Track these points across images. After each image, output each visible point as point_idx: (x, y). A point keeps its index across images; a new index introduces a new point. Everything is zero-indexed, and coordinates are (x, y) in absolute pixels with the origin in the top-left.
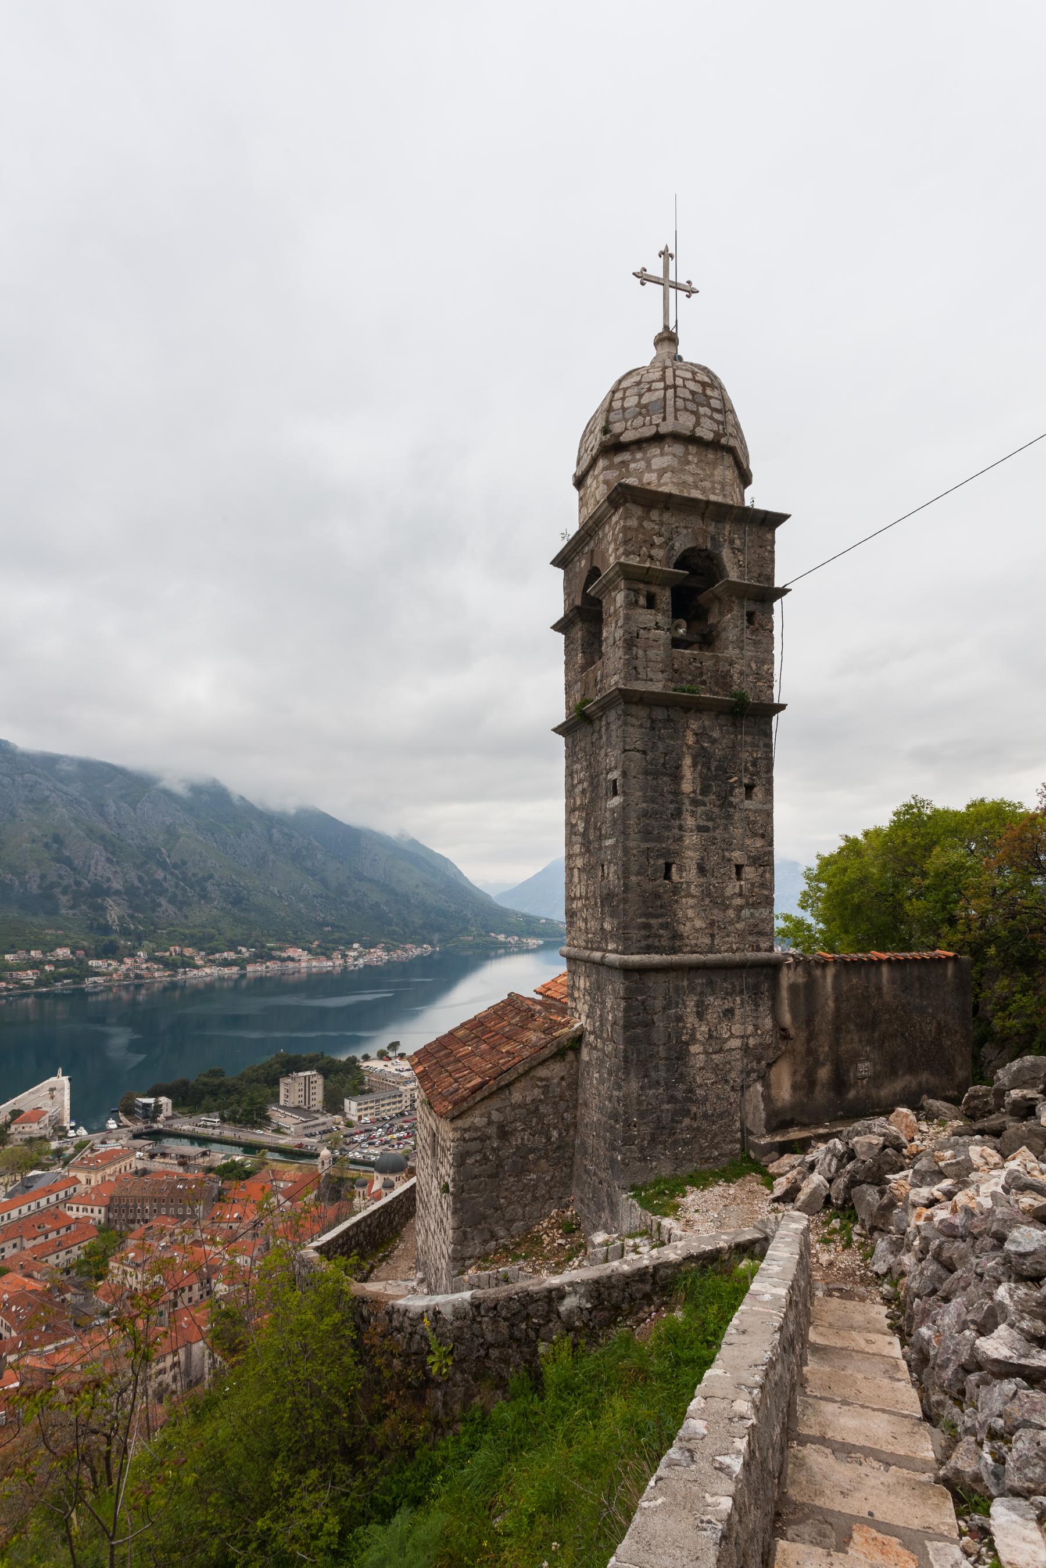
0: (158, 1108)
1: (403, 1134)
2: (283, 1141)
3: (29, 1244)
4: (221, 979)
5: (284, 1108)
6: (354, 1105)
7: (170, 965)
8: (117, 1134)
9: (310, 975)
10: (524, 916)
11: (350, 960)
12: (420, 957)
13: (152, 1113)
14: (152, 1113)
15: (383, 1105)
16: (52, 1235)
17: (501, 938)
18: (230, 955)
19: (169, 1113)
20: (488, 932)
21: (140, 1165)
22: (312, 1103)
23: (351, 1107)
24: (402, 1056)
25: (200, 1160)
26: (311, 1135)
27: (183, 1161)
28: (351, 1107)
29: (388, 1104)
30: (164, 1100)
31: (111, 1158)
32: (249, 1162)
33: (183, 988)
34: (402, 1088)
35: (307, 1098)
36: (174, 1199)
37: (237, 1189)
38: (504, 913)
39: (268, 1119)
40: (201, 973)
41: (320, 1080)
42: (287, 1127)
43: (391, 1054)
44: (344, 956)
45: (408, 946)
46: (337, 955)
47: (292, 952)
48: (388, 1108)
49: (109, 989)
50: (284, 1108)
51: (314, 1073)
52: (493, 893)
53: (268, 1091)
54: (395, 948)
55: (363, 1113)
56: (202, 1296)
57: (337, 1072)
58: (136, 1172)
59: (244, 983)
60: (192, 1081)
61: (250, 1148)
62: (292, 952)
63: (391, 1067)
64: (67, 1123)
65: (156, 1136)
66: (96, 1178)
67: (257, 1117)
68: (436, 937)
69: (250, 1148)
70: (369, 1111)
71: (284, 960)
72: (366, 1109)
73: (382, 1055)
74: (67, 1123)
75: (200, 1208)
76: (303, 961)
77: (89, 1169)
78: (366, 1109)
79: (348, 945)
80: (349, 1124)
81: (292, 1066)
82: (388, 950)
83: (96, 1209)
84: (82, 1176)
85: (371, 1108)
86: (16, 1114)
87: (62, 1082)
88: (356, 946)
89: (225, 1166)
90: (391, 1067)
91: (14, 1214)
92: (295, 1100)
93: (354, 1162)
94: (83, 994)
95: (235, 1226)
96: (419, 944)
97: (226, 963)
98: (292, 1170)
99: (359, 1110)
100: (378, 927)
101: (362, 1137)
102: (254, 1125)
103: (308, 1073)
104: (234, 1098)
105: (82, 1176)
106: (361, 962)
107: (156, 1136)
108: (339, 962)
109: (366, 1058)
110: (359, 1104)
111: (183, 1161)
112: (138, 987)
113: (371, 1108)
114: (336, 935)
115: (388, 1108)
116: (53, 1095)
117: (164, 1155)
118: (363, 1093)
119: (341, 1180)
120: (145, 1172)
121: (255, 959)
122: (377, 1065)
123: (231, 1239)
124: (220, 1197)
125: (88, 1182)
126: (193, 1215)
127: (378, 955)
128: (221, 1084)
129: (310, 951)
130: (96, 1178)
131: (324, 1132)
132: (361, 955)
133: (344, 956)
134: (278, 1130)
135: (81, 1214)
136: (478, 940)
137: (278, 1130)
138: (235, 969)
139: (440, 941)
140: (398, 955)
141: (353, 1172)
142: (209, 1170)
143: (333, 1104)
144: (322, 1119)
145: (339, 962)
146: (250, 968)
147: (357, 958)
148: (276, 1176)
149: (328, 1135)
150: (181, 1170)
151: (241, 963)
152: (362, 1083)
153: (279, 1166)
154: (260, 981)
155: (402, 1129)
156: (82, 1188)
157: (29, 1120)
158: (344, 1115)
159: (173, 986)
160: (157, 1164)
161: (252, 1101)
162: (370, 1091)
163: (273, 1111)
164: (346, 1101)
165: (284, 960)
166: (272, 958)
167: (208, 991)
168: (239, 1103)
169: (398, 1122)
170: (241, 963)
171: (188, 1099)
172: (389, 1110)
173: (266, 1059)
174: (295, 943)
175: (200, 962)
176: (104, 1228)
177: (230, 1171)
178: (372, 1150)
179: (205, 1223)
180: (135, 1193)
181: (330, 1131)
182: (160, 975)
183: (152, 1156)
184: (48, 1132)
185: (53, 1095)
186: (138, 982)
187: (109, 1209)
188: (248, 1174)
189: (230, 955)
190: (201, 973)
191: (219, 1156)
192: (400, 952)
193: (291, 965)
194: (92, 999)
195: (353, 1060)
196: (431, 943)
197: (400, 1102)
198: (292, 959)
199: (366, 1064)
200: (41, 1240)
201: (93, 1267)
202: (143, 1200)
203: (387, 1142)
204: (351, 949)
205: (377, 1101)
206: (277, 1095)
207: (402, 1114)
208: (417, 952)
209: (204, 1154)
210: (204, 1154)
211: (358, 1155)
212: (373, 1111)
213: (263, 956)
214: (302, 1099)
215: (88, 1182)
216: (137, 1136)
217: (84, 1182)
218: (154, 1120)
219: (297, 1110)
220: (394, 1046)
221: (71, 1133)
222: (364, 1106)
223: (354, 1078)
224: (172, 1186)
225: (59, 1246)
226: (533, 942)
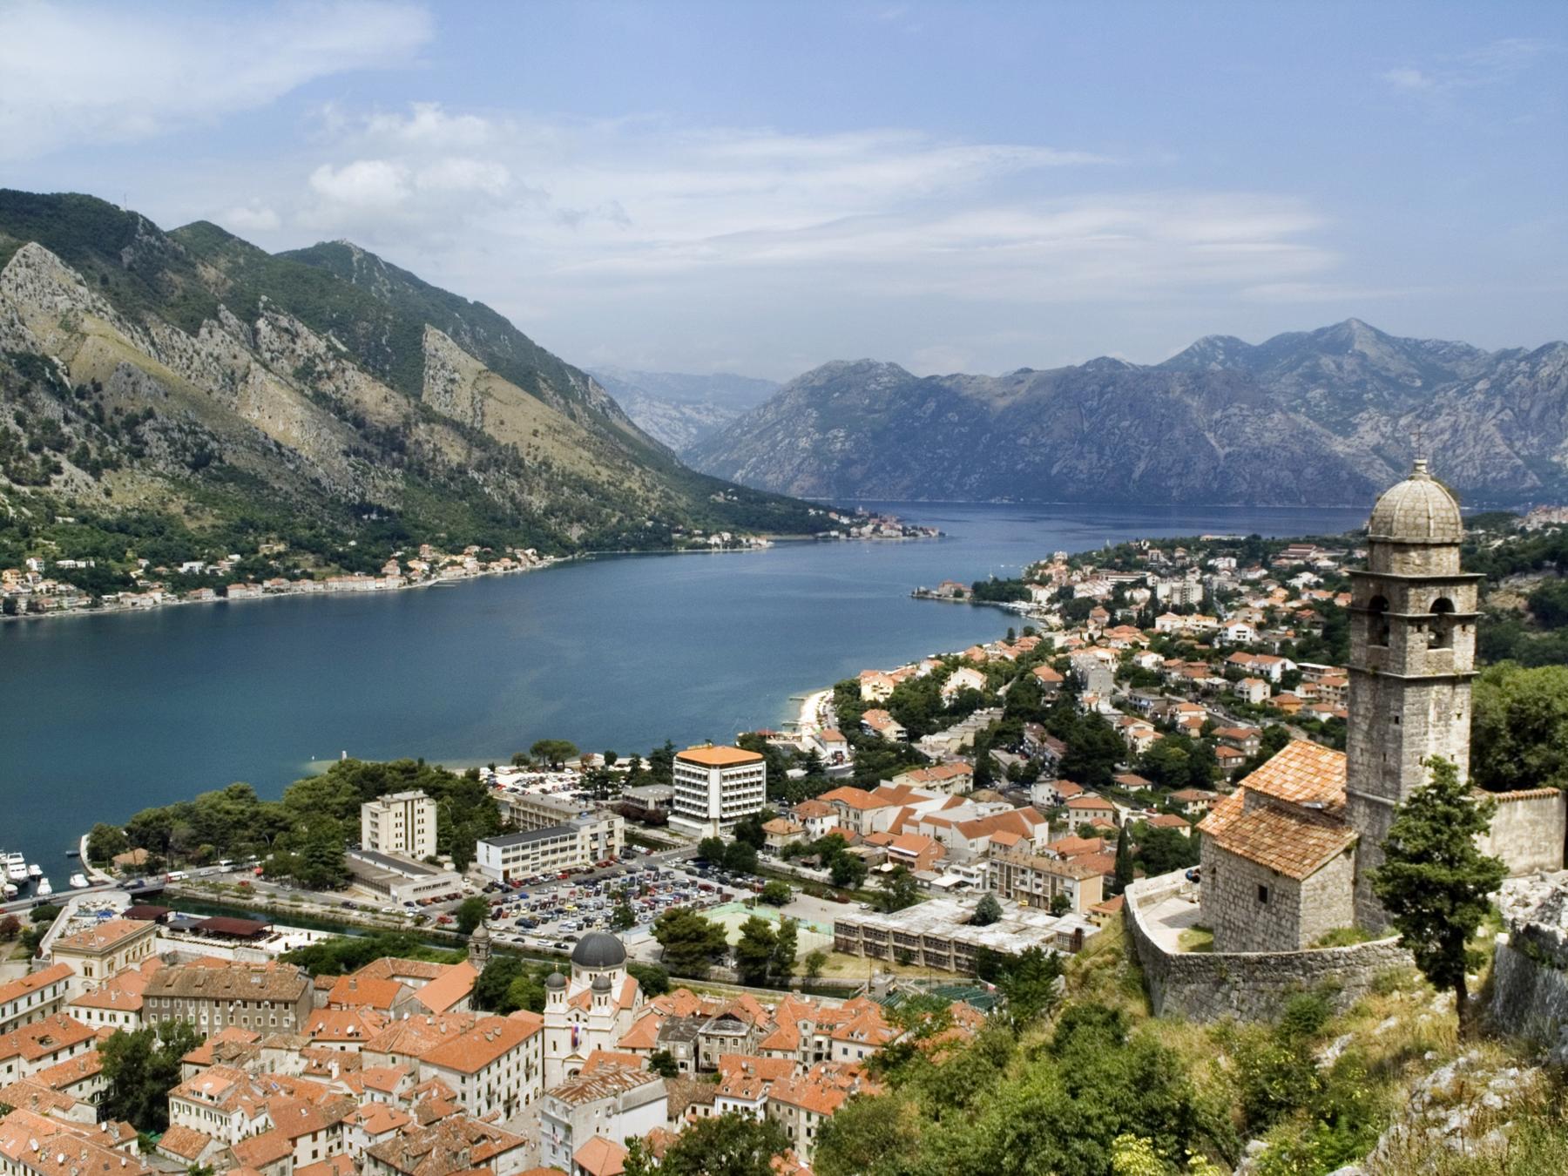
6: (496, 853)
15: (545, 853)
22: (418, 847)
29: (554, 851)
35: (410, 838)
44: (405, 570)
46: (391, 567)
48: (554, 857)
51: (421, 793)
55: (510, 866)
56: (331, 1149)
58: (164, 957)
67: (327, 871)
70: (521, 863)
72: (516, 859)
78: (516, 859)
81: (375, 785)
83: (120, 1016)
85: (525, 857)
99: (505, 861)
103: (408, 795)
105: (76, 964)
110: (504, 851)
113: (525, 857)
115: (554, 857)
121: (240, 575)
125: (88, 971)
156: (77, 988)
192: (507, 562)
197: (573, 848)
200: (48, 1062)
205: (535, 846)
212: (528, 862)
214: (402, 840)
215: (88, 971)
217: (80, 971)
222: (511, 855)
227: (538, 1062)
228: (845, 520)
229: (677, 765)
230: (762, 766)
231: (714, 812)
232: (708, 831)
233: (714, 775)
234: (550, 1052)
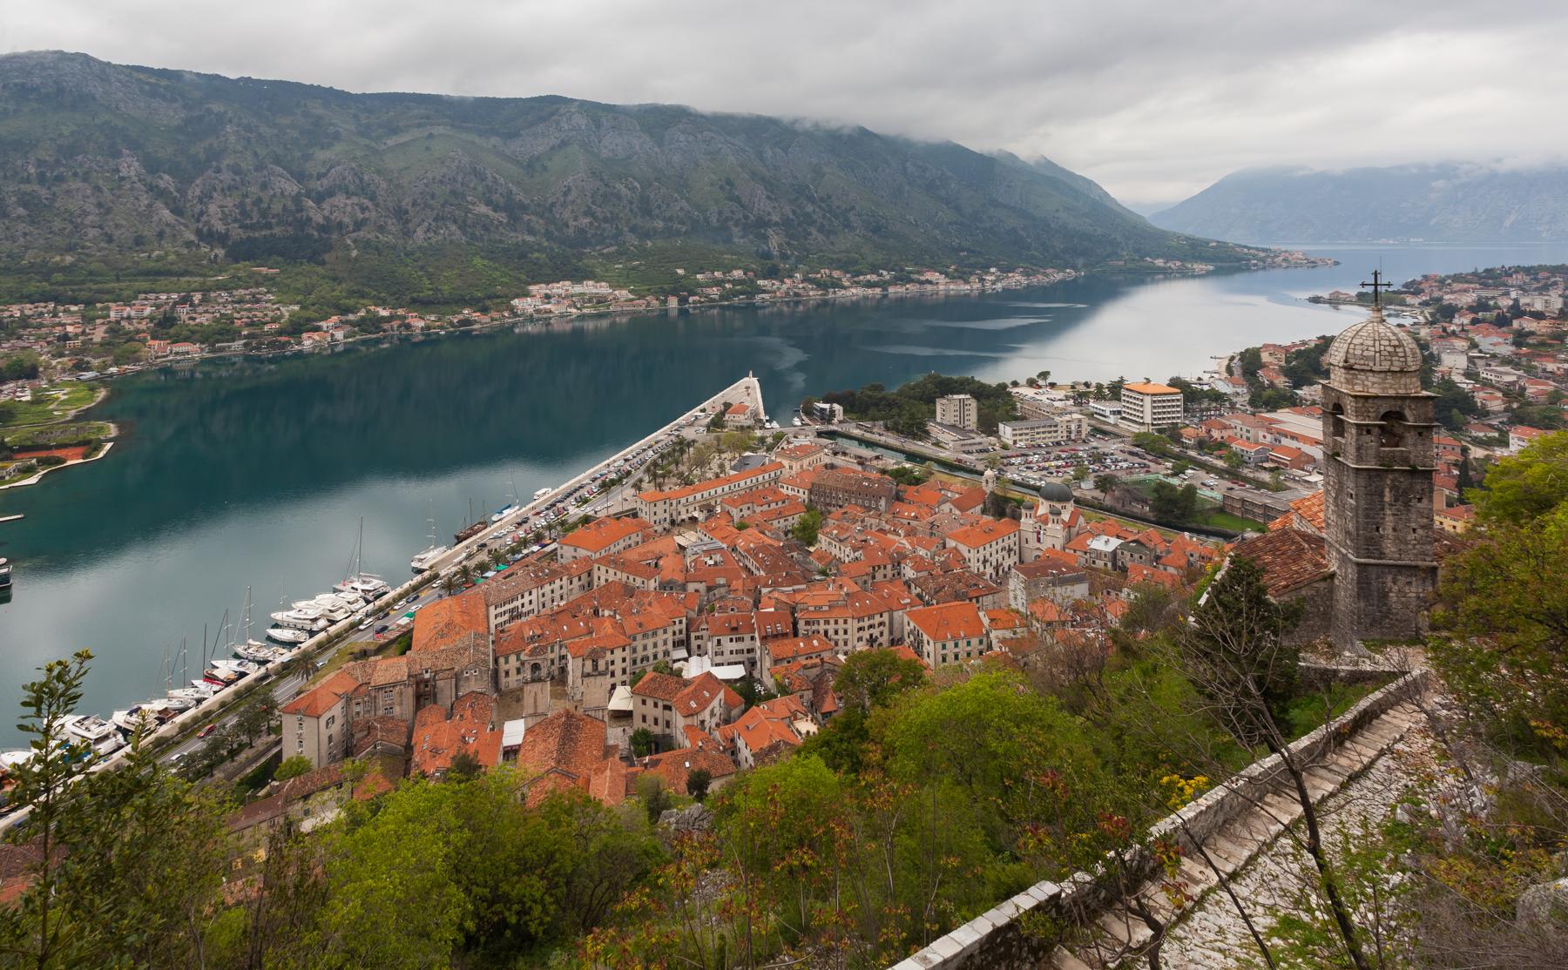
0: (832, 413)
1: (1060, 463)
2: (943, 455)
3: (758, 509)
4: (866, 298)
5: (941, 424)
6: (1008, 430)
7: (820, 285)
8: (802, 433)
9: (947, 296)
10: (1187, 238)
11: (988, 285)
12: (1062, 282)
13: (827, 417)
14: (827, 417)
16: (773, 506)
17: (1160, 262)
18: (873, 278)
19: (841, 417)
20: (1142, 258)
21: (827, 460)
23: (1006, 431)
24: (1053, 385)
25: (875, 462)
26: (969, 453)
27: (861, 461)
28: (1006, 431)
30: (836, 407)
31: (805, 451)
32: (917, 470)
33: (834, 305)
34: (1057, 419)
35: (962, 417)
36: (863, 495)
37: (910, 491)
38: (1162, 236)
39: (927, 433)
40: (848, 293)
41: (973, 404)
42: (945, 442)
43: (1041, 383)
44: (982, 280)
45: (1049, 271)
47: (929, 276)
49: (774, 303)
50: (941, 424)
52: (1146, 215)
53: (925, 408)
54: (1035, 273)
57: (988, 397)
58: (826, 466)
59: (886, 302)
60: (858, 394)
61: (911, 456)
62: (929, 276)
63: (1044, 396)
64: (764, 417)
65: (832, 435)
66: (796, 466)
68: (1080, 261)
69: (911, 456)
71: (922, 283)
73: (1031, 383)
74: (764, 417)
75: (883, 502)
76: (941, 284)
77: (791, 458)
79: (985, 268)
80: (1005, 447)
81: (947, 388)
82: (1027, 275)
84: (786, 463)
86: (727, 406)
87: (752, 381)
88: (993, 270)
89: (897, 471)
90: (1044, 396)
91: (742, 484)
92: (951, 418)
93: (1014, 483)
94: (752, 308)
95: (914, 523)
96: (1061, 268)
97: (870, 285)
98: (958, 482)
100: (1014, 252)
101: (1019, 460)
102: (915, 437)
104: (895, 411)
105: (786, 463)
106: (999, 286)
107: (832, 435)
108: (977, 286)
109: (1015, 384)
111: (861, 461)
112: (797, 303)
114: (972, 260)
116: (747, 392)
117: (845, 454)
118: (1016, 419)
119: (1007, 500)
120: (832, 467)
122: (1029, 392)
123: (911, 533)
124: (898, 498)
126: (877, 509)
127: (1017, 279)
128: (883, 398)
129: (947, 275)
130: (796, 466)
131: (981, 451)
132: (998, 280)
133: (982, 280)
134: (937, 444)
135: (790, 493)
136: (1130, 265)
137: (937, 444)
138: (878, 290)
139: (1085, 266)
140: (1038, 279)
141: (1015, 494)
142: (884, 472)
143: (988, 425)
144: (978, 439)
145: (977, 286)
146: (891, 290)
147: (994, 281)
148: (945, 486)
149: (985, 455)
150: (859, 468)
151: (883, 285)
152: (1015, 409)
153: (944, 477)
154: (901, 300)
155: (1058, 458)
156: (786, 471)
157: (736, 412)
158: (999, 437)
159: (825, 303)
160: (839, 461)
161: (912, 416)
162: (1023, 418)
163: (932, 428)
164: (1001, 426)
165: (922, 283)
166: (912, 281)
167: (855, 307)
168: (899, 415)
169: (1056, 452)
170: (883, 285)
171: (857, 407)
172: (1045, 439)
173: (920, 378)
174: (932, 268)
175: (847, 284)
176: (810, 507)
177: (900, 475)
178: (1030, 474)
179: (889, 516)
180: (830, 483)
181: (986, 451)
182: (814, 294)
183: (835, 454)
184: (751, 422)
185: (747, 392)
186: (797, 299)
187: (811, 492)
188: (917, 481)
189: (873, 278)
190: (848, 293)
191: (891, 462)
193: (929, 287)
194: (760, 312)
195: (1003, 387)
196: (1074, 268)
198: (930, 282)
199: (1015, 390)
200: (765, 508)
201: (807, 535)
202: (837, 489)
203: (1044, 469)
204: (988, 273)
206: (934, 412)
207: (1058, 444)
208: (1059, 276)
209: (877, 458)
210: (877, 458)
211: (1016, 477)
213: (903, 279)
216: (820, 434)
218: (829, 422)
219: (953, 427)
220: (1044, 375)
221: (767, 425)
223: (1006, 404)
224: (859, 482)
225: (780, 515)
226: (1199, 267)
227: (1016, 548)
228: (1262, 254)
229: (1123, 392)
230: (1181, 396)
231: (1148, 420)
232: (1143, 429)
233: (1148, 400)
234: (1024, 544)
